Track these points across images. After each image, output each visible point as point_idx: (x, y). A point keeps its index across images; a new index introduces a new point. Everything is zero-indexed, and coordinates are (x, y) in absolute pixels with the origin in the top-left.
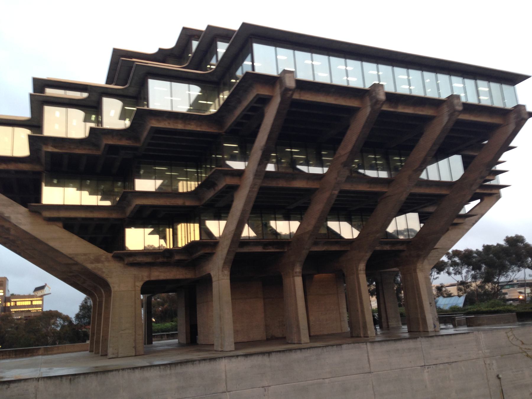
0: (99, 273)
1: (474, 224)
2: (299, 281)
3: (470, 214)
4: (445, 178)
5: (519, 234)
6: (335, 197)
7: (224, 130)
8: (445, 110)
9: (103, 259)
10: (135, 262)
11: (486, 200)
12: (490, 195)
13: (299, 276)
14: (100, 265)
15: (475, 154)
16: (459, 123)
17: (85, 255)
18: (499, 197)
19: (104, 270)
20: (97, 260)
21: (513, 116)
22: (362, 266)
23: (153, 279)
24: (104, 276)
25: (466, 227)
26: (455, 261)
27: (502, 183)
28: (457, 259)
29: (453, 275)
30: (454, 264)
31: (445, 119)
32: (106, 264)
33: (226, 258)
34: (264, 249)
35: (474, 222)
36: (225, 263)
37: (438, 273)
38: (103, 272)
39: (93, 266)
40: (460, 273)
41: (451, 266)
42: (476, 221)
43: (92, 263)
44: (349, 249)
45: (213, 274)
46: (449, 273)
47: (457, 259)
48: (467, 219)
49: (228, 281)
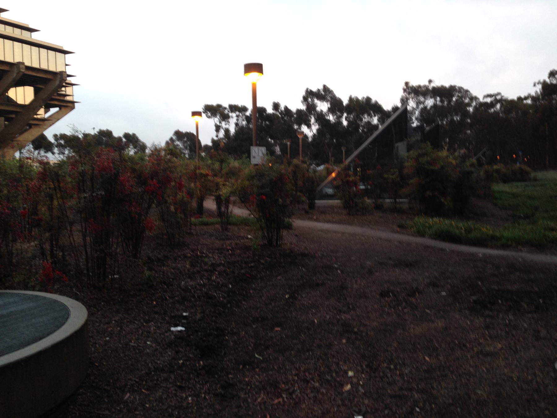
1: (51, 125)
3: (47, 119)
4: (20, 101)
5: (110, 129)
8: (15, 69)
11: (63, 109)
12: (67, 106)
15: (43, 87)
16: (24, 75)
18: (73, 108)
21: (59, 76)
25: (45, 127)
26: (61, 143)
27: (75, 100)
28: (62, 142)
29: (57, 155)
30: (59, 146)
31: (15, 75)
35: (51, 124)
37: (46, 152)
40: (64, 154)
41: (57, 147)
42: (53, 124)
46: (53, 153)
47: (62, 142)
48: (46, 122)
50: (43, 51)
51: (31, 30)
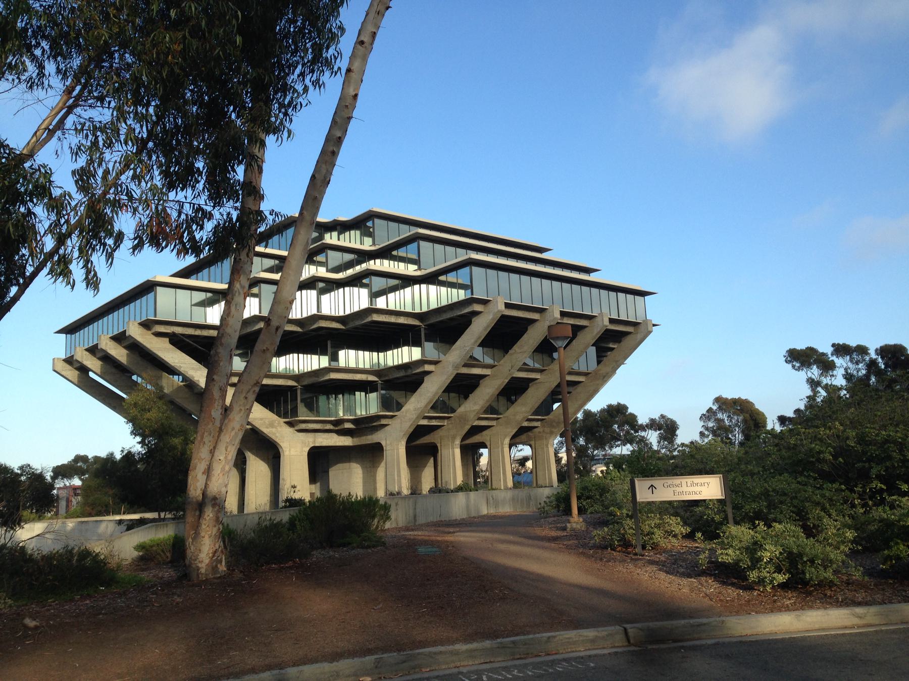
0: (273, 437)
2: (458, 452)
6: (505, 384)
7: (421, 324)
9: (276, 424)
10: (307, 428)
13: (457, 448)
14: (274, 430)
17: (261, 419)
19: (277, 435)
20: (271, 425)
22: (507, 441)
23: (317, 445)
24: (277, 440)
32: (279, 429)
33: (407, 430)
34: (428, 422)
36: (404, 435)
38: (277, 437)
39: (268, 430)
43: (267, 428)
44: (495, 424)
45: (383, 443)
49: (404, 450)
50: (621, 296)
51: (588, 271)
